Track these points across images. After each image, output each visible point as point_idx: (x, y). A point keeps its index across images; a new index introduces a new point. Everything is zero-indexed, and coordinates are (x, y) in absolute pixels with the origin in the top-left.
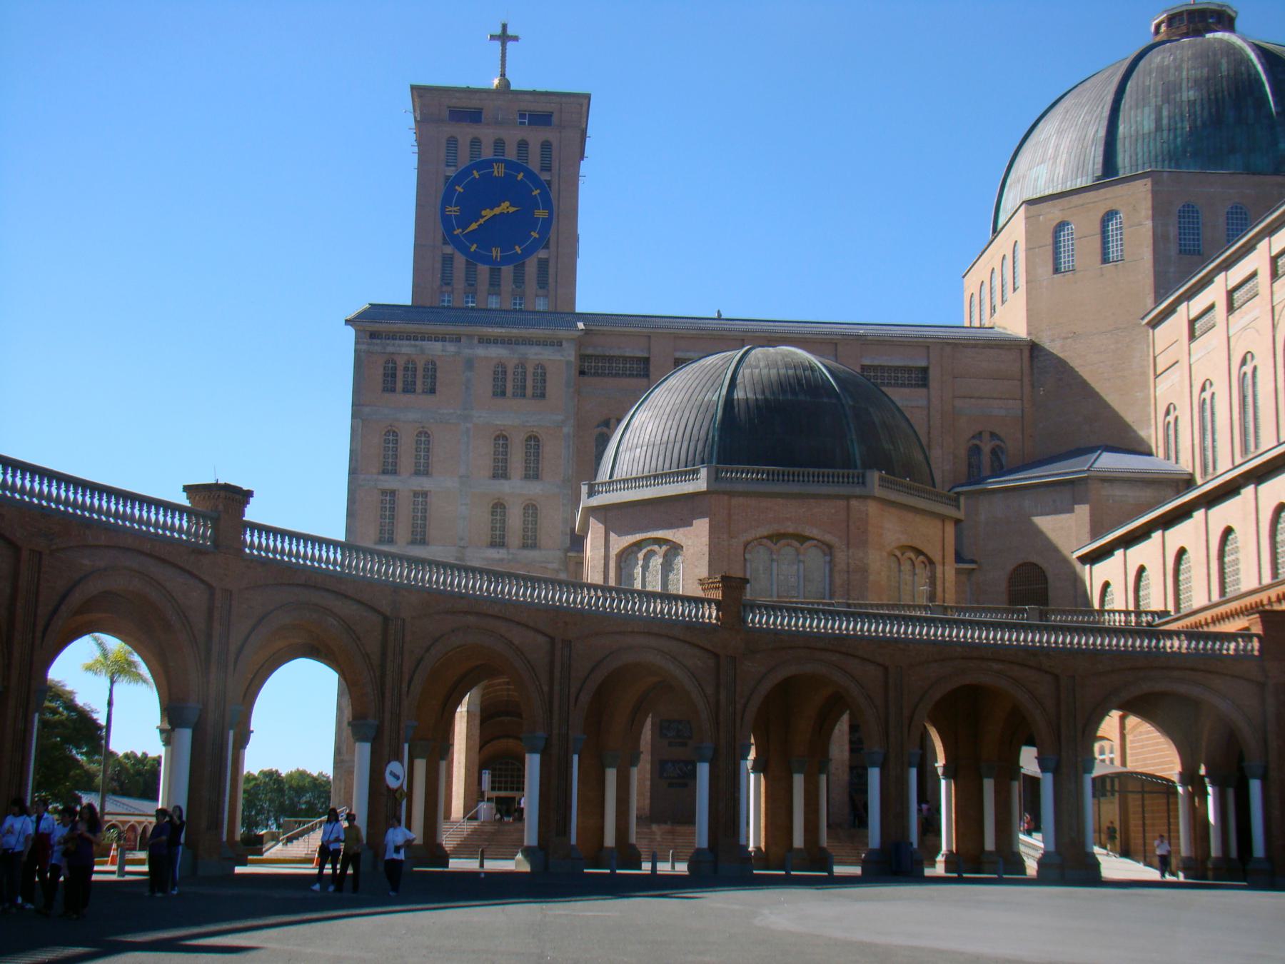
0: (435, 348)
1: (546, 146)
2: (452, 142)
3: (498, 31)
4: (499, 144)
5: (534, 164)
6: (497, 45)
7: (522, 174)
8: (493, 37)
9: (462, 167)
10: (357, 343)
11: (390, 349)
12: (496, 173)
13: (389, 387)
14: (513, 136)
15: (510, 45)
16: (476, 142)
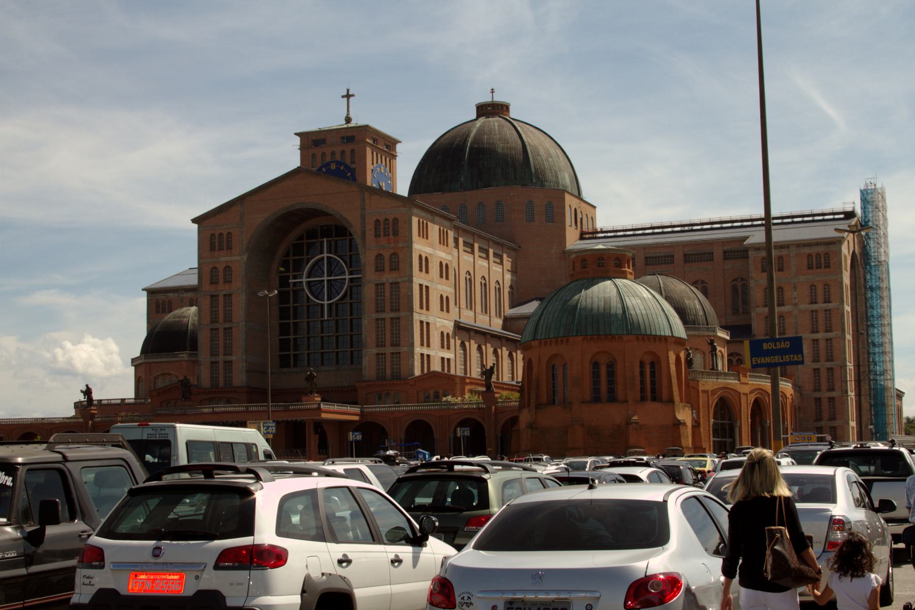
0: (171, 295)
1: (353, 151)
2: (314, 155)
3: (345, 93)
4: (333, 153)
5: (348, 162)
6: (345, 99)
7: (343, 167)
8: (343, 97)
9: (318, 167)
10: (147, 296)
11: (158, 297)
12: (332, 168)
13: (157, 312)
14: (338, 150)
15: (351, 99)
16: (323, 154)
